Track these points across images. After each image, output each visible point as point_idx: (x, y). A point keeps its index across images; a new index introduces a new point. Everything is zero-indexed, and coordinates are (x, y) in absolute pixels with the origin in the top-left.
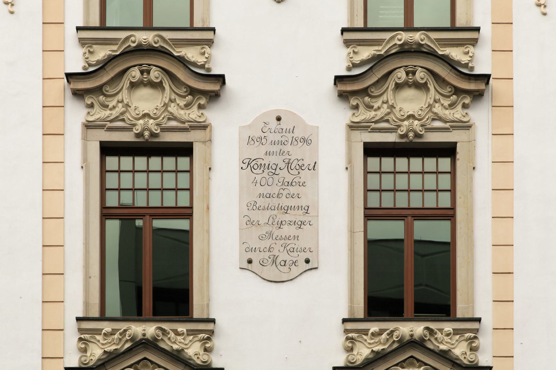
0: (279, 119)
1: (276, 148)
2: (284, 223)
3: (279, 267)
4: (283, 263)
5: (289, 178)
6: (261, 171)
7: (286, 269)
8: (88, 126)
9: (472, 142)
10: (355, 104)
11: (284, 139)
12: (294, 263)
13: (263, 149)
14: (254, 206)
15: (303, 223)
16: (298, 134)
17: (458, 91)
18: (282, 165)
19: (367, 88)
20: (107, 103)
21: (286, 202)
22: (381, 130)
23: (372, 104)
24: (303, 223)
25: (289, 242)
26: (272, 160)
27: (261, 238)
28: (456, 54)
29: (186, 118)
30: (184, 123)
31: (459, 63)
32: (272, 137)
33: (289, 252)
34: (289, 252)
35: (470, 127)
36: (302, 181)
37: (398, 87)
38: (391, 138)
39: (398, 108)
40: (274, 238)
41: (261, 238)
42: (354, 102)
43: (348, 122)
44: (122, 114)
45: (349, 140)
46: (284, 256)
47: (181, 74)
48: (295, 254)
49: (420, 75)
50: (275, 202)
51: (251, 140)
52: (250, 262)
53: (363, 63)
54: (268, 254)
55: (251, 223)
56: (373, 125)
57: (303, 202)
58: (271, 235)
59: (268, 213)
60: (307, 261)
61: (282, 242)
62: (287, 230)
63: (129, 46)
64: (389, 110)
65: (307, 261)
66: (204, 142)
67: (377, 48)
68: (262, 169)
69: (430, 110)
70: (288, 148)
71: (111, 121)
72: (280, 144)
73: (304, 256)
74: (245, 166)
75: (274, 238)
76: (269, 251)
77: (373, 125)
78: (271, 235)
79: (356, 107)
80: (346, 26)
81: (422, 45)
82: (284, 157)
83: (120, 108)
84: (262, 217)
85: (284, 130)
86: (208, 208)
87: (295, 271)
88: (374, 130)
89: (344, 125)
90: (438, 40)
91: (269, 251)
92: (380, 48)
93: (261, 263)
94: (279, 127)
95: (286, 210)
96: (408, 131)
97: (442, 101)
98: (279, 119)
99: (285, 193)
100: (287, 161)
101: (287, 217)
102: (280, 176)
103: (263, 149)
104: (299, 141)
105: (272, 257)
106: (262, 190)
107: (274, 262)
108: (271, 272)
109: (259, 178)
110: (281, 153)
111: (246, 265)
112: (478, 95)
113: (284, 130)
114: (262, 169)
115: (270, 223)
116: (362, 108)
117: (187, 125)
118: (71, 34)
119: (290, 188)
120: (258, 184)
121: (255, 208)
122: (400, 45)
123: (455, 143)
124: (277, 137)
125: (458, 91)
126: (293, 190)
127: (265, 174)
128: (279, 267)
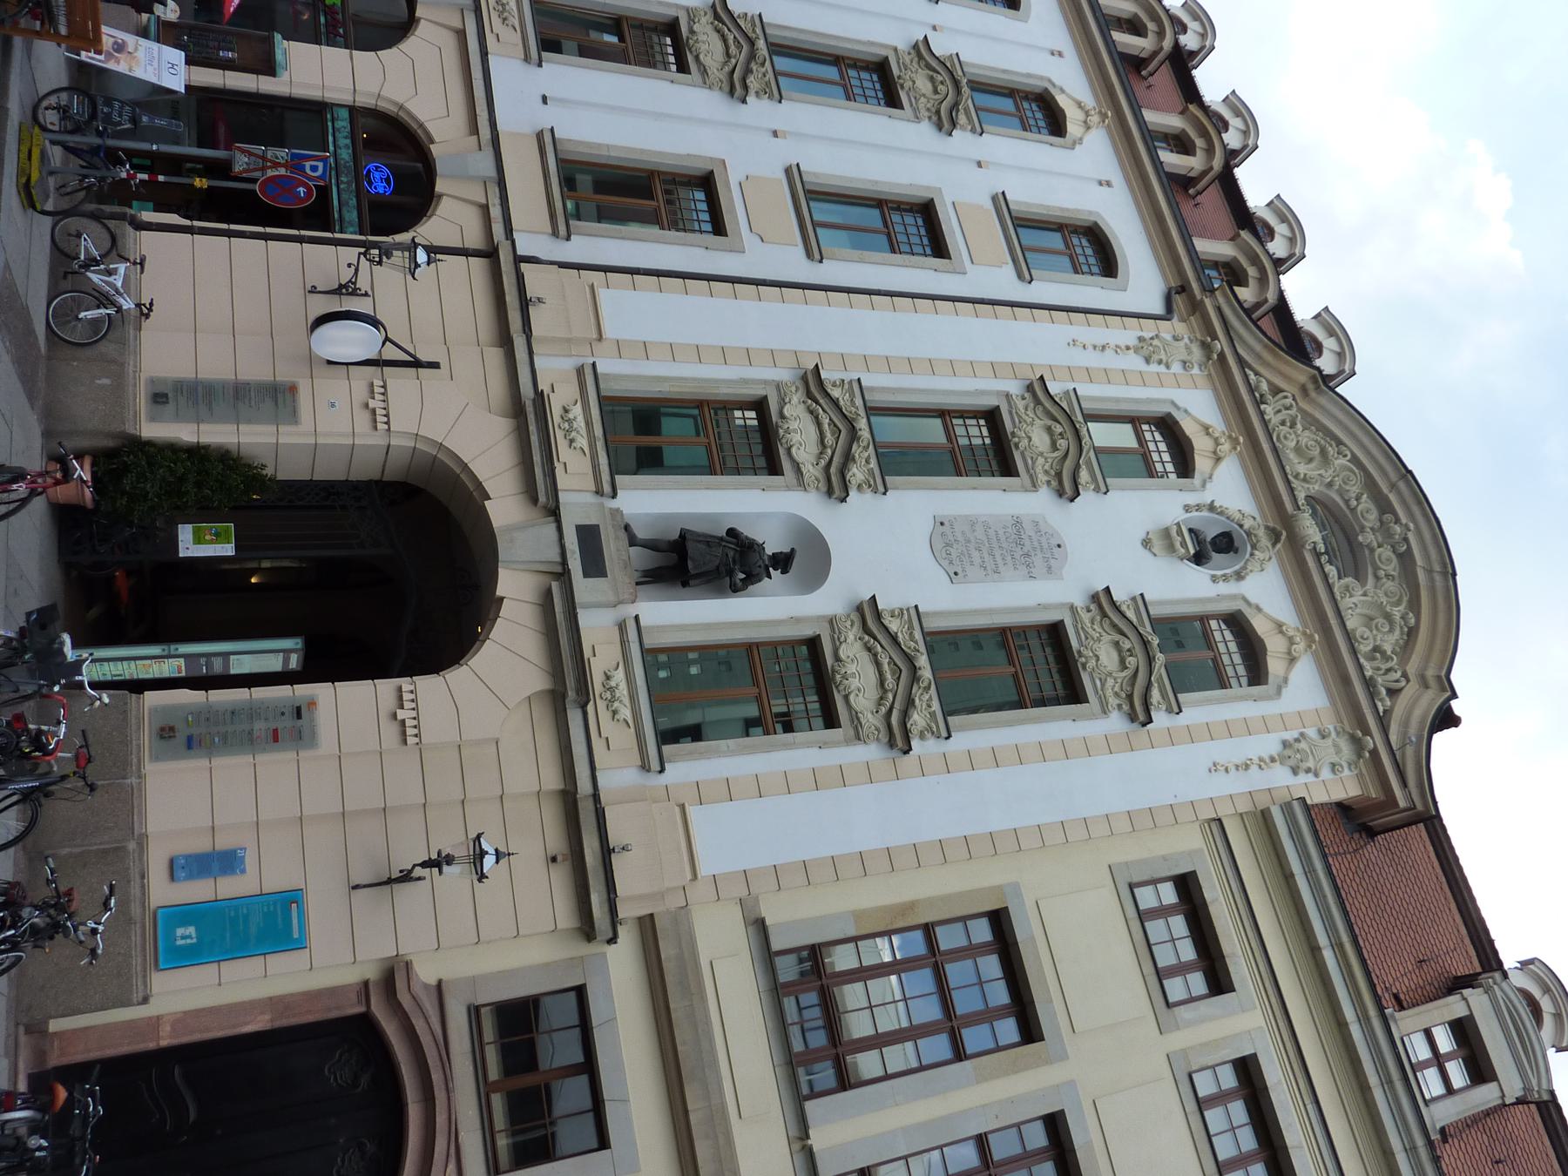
0: (1059, 546)
5: (1017, 556)
7: (944, 555)
8: (1008, 396)
9: (1092, 717)
12: (951, 563)
13: (1032, 533)
14: (986, 527)
15: (985, 568)
18: (1025, 549)
20: (1029, 409)
21: (997, 553)
22: (1077, 633)
24: (985, 568)
26: (1027, 542)
27: (963, 533)
29: (1038, 471)
32: (1043, 540)
35: (1105, 713)
37: (1117, 644)
41: (963, 533)
42: (1093, 607)
43: (1075, 605)
44: (1025, 421)
45: (1062, 605)
46: (954, 556)
47: (1069, 464)
49: (1131, 661)
50: (995, 545)
51: (1037, 524)
52: (942, 524)
54: (952, 539)
55: (973, 523)
56: (1080, 626)
57: (1002, 568)
59: (985, 538)
60: (956, 574)
62: (976, 554)
64: (1096, 638)
66: (1023, 486)
70: (1038, 552)
71: (1016, 413)
73: (959, 572)
76: (955, 540)
77: (1080, 626)
78: (969, 541)
79: (1089, 611)
83: (1029, 420)
84: (980, 533)
86: (975, 489)
87: (945, 563)
88: (1076, 627)
89: (1072, 601)
90: (1161, 675)
91: (955, 540)
96: (1086, 658)
97: (1117, 685)
99: (1004, 552)
101: (986, 555)
103: (1032, 533)
106: (1001, 532)
107: (947, 545)
108: (938, 546)
109: (1010, 530)
111: (939, 520)
112: (1133, 717)
117: (1032, 471)
118: (1070, 386)
122: (1148, 641)
124: (1045, 546)
125: (1130, 697)
127: (1014, 536)
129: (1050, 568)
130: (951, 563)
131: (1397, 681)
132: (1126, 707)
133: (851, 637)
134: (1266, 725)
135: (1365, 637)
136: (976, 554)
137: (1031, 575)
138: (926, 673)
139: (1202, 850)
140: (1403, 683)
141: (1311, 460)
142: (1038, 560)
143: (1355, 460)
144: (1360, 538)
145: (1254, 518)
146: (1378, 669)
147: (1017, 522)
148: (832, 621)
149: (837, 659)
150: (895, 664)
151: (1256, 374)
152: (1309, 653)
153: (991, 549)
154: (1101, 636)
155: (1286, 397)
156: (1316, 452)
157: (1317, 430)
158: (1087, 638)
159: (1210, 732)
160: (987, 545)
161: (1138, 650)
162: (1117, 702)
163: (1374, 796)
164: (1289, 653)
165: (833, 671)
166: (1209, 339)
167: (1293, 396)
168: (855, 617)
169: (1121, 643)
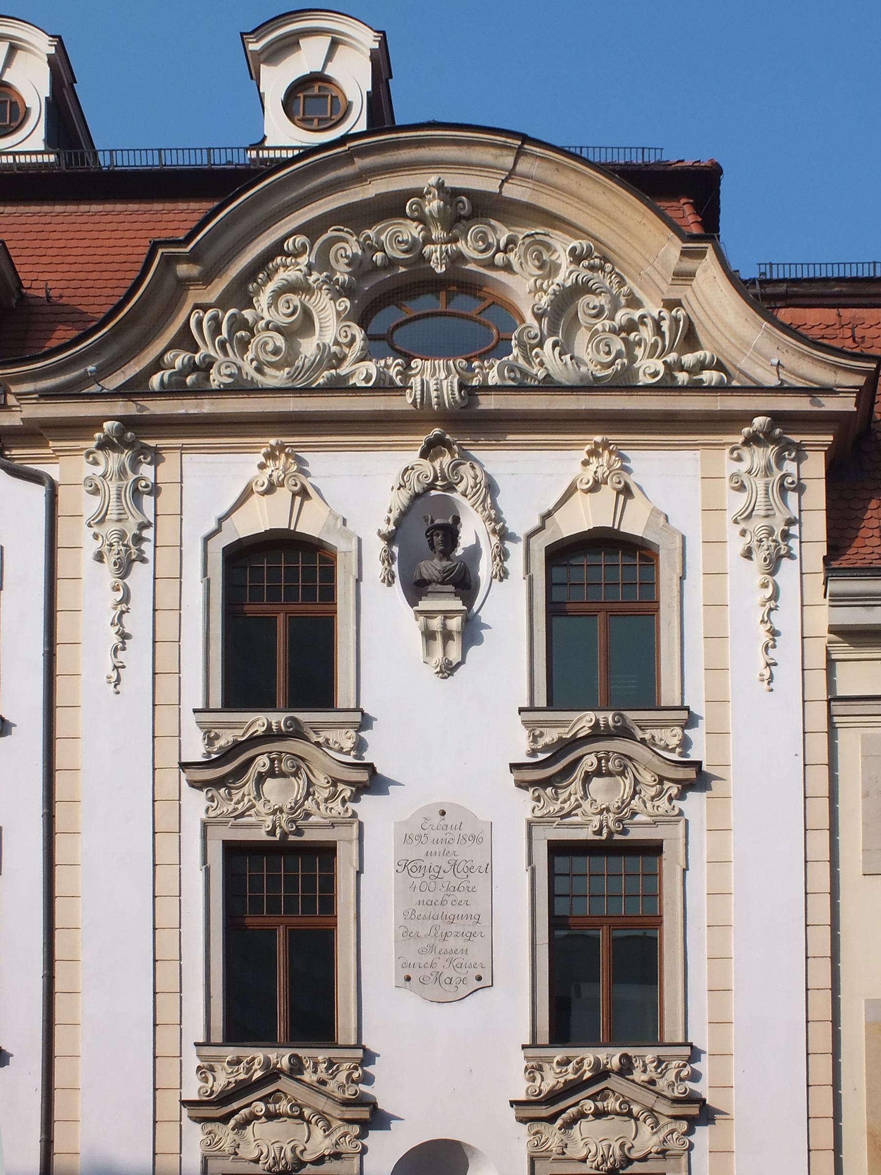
0: (443, 813)
1: (439, 848)
2: (449, 934)
3: (443, 985)
4: (448, 981)
5: (455, 882)
6: (420, 875)
7: (452, 988)
11: (448, 837)
12: (463, 981)
13: (424, 849)
14: (410, 915)
15: (473, 934)
16: (467, 831)
18: (447, 867)
21: (450, 910)
24: (473, 934)
25: (457, 956)
26: (435, 861)
27: (421, 952)
30: (326, 818)
32: (434, 835)
33: (456, 968)
34: (456, 968)
36: (471, 885)
40: (437, 951)
41: (421, 952)
46: (448, 973)
48: (463, 970)
50: (439, 909)
51: (408, 838)
52: (408, 979)
53: (546, 748)
57: (473, 910)
58: (433, 948)
59: (431, 923)
61: (447, 956)
62: (452, 943)
63: (257, 731)
65: (479, 978)
67: (561, 730)
68: (422, 872)
70: (454, 847)
72: (444, 842)
73: (476, 972)
74: (400, 869)
75: (437, 951)
78: (433, 948)
82: (449, 858)
84: (423, 928)
85: (449, 827)
87: (464, 990)
92: (567, 730)
93: (421, 980)
94: (442, 823)
95: (452, 920)
98: (443, 813)
99: (450, 899)
100: (452, 862)
101: (453, 928)
102: (445, 879)
103: (424, 849)
104: (467, 839)
105: (435, 974)
106: (421, 896)
109: (417, 882)
110: (445, 853)
113: (449, 827)
114: (422, 872)
115: (432, 934)
119: (457, 893)
120: (417, 889)
121: (413, 917)
123: (662, 841)
124: (440, 835)
126: (459, 896)
127: (426, 878)
128: (443, 985)
129: (474, 838)
130: (463, 981)
131: (676, 320)
134: (714, 574)
135: (607, 349)
136: (452, 943)
137: (483, 869)
139: (864, 737)
140: (681, 314)
141: (307, 315)
142: (465, 853)
143: (312, 229)
144: (439, 270)
145: (406, 470)
146: (655, 345)
147: (406, 867)
151: (157, 365)
153: (444, 917)
155: (199, 322)
156: (295, 299)
157: (255, 281)
159: (715, 669)
160: (439, 921)
163: (831, 438)
166: (97, 435)
167: (196, 306)
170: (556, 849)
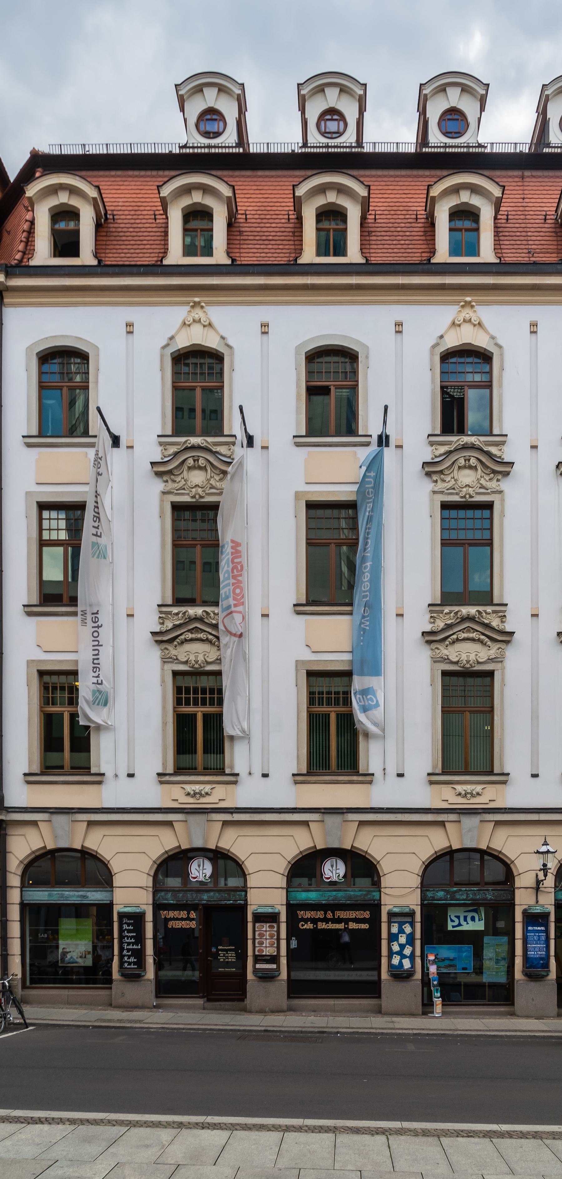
10: (435, 479)
17: (494, 472)
19: (442, 470)
23: (445, 479)
28: (494, 450)
31: (495, 456)
38: (456, 498)
39: (460, 481)
49: (473, 462)
69: (479, 482)
80: (430, 433)
81: (475, 445)
112: (507, 474)
116: (439, 482)
125: (494, 472)
132: (500, 477)
133: (445, 652)
138: (472, 610)
148: (435, 661)
149: (457, 663)
150: (464, 629)
152: (477, 308)
154: (454, 478)
158: (454, 489)
161: (467, 453)
162: (495, 480)
164: (475, 325)
165: (463, 667)
168: (434, 646)
169: (460, 465)
170: (445, 506)
